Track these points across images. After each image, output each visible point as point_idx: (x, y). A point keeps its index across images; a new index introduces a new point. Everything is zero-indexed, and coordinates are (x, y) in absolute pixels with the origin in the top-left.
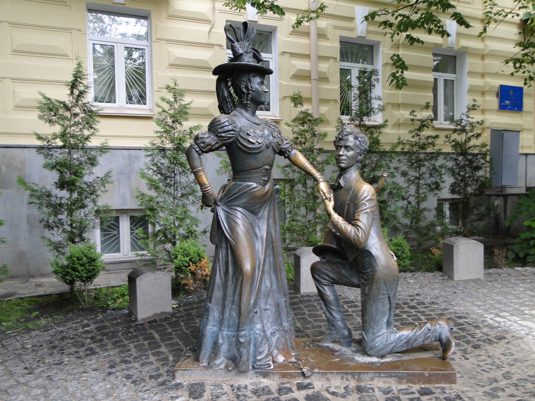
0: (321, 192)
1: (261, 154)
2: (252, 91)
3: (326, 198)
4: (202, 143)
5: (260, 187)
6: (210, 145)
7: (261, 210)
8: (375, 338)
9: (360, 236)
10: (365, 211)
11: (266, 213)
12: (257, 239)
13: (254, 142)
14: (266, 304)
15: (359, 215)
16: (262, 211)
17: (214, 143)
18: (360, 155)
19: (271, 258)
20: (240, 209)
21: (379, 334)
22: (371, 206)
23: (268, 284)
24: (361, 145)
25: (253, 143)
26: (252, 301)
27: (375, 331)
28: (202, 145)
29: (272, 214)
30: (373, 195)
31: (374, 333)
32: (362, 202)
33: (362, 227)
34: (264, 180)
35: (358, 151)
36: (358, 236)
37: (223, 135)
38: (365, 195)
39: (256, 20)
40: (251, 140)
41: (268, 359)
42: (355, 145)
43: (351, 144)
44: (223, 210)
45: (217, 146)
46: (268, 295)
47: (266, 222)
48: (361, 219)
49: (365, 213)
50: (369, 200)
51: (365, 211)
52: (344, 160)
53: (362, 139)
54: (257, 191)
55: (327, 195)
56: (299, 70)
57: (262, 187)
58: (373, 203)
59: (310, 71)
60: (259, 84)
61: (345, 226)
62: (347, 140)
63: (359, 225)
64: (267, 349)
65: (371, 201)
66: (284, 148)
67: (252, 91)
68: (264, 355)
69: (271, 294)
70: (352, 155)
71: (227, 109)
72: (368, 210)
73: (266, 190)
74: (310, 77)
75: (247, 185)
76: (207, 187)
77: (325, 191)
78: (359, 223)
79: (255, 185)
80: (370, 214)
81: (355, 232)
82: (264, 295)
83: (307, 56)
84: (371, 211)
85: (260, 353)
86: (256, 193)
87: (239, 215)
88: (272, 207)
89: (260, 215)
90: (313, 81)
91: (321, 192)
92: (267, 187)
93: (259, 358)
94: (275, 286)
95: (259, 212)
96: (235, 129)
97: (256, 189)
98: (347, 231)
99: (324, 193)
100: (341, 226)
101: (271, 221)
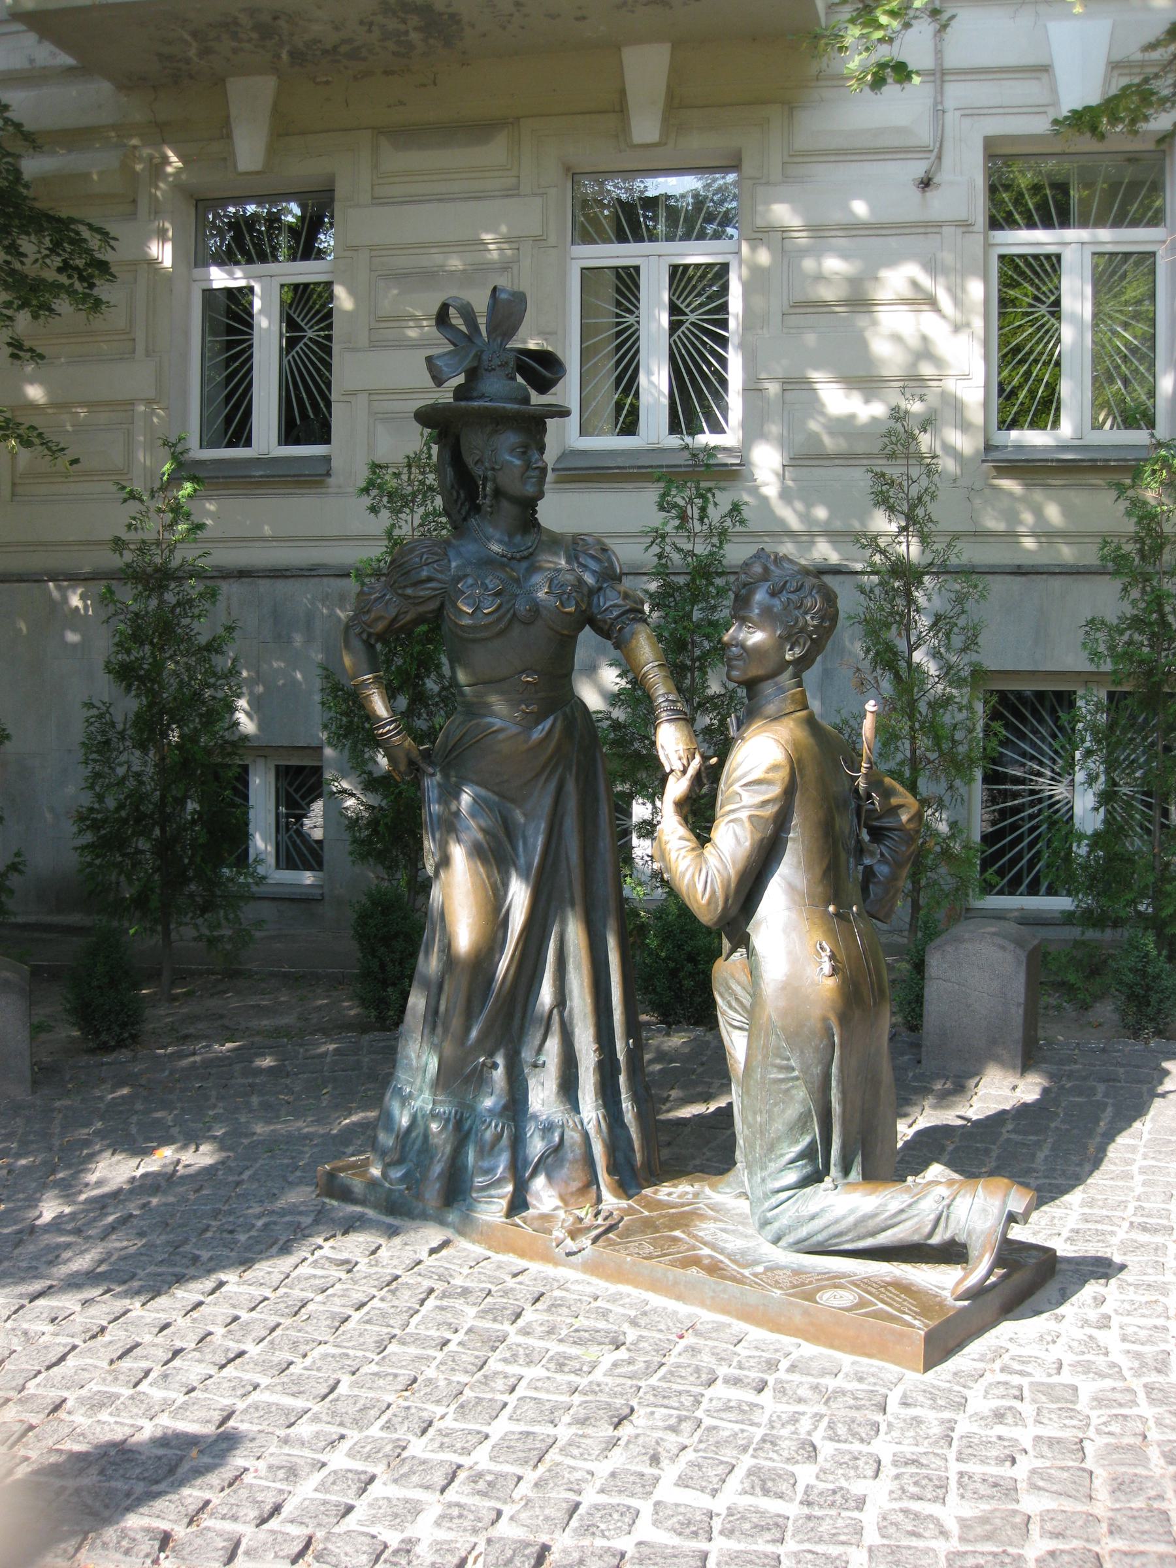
11: (547, 801)
30: (775, 768)
34: (524, 712)
37: (409, 591)
50: (759, 782)
65: (763, 787)
76: (383, 726)
80: (747, 824)
84: (750, 817)
88: (571, 787)
96: (440, 576)
97: (501, 736)
101: (571, 824)
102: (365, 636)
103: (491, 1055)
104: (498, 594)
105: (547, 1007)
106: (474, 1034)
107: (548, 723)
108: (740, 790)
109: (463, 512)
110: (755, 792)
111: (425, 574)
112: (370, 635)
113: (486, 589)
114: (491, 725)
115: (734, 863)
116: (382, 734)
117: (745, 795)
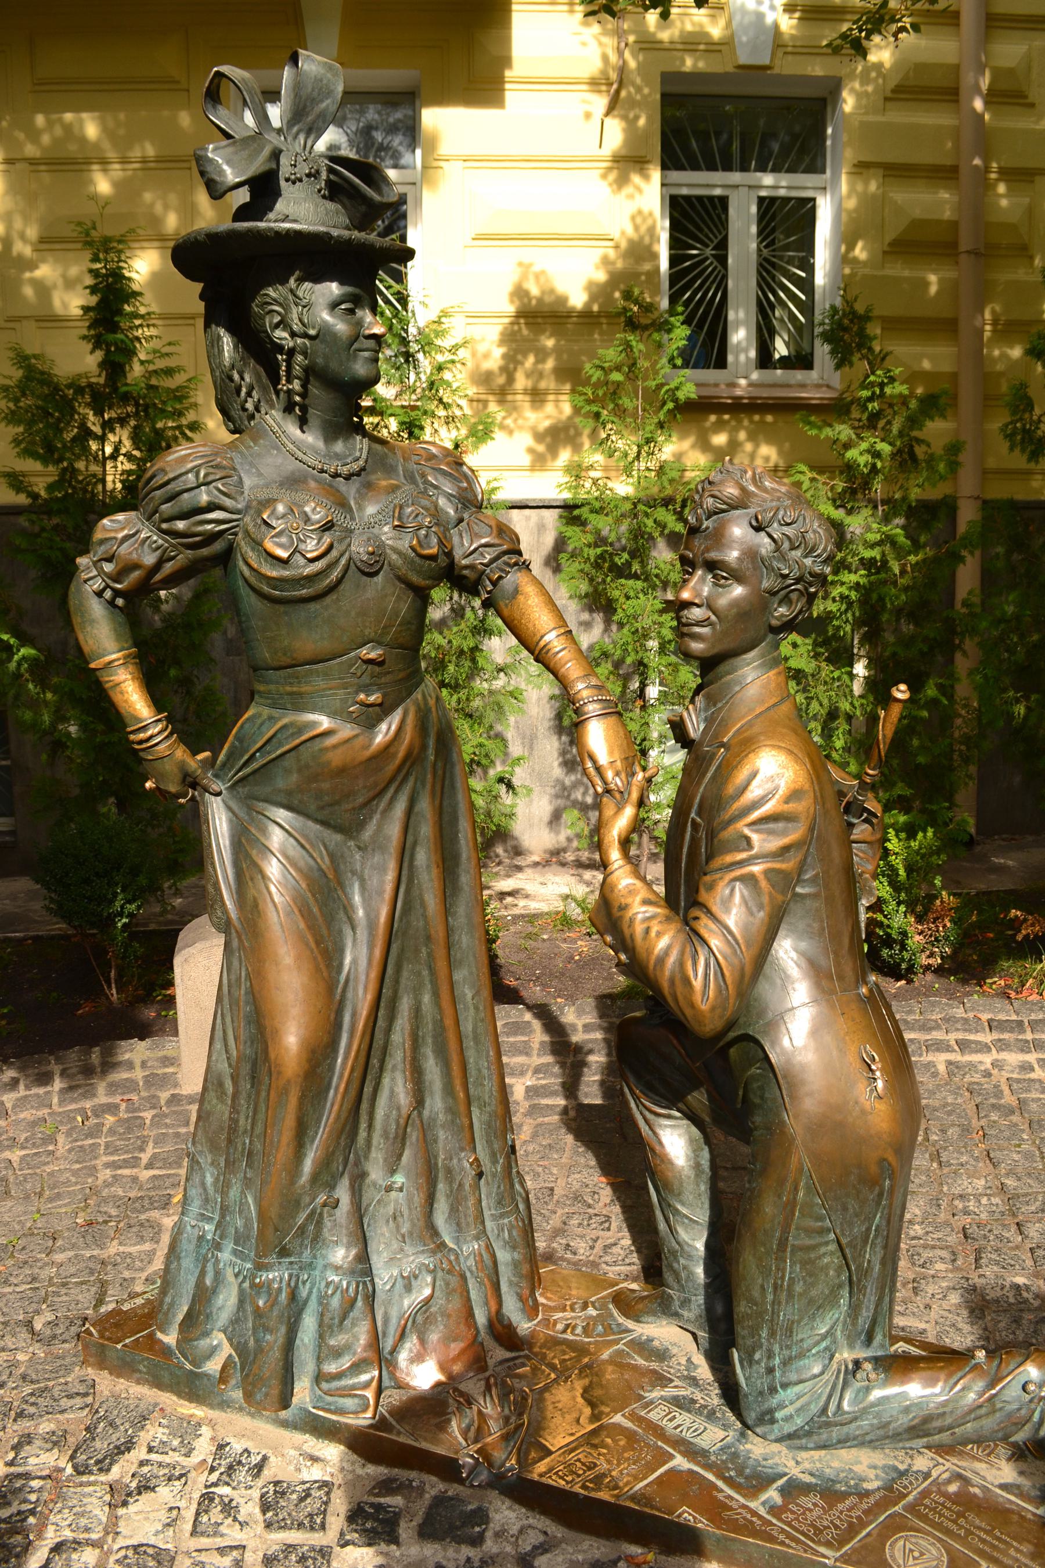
0: (589, 764)
1: (328, 600)
2: (306, 336)
3: (608, 791)
4: (109, 560)
5: (347, 731)
6: (136, 566)
7: (373, 812)
8: (773, 1390)
9: (698, 984)
10: (738, 873)
11: (394, 830)
12: (353, 929)
13: (284, 554)
14: (393, 1172)
15: (711, 887)
16: (377, 817)
17: (149, 559)
18: (786, 600)
19: (426, 998)
20: (282, 815)
21: (793, 1377)
22: (775, 844)
23: (404, 1099)
24: (783, 558)
25: (284, 562)
26: (308, 1166)
27: (777, 1361)
28: (108, 567)
29: (426, 830)
30: (794, 795)
31: (770, 1371)
32: (731, 829)
33: (715, 943)
34: (363, 704)
35: (765, 584)
36: (687, 982)
37: (181, 525)
38: (755, 791)
39: (766, 61)
40: (269, 545)
41: (364, 1377)
42: (751, 554)
43: (733, 555)
44: (229, 808)
45: (168, 567)
46: (401, 1138)
47: (392, 865)
48: (715, 909)
49: (741, 879)
51: (738, 873)
52: (698, 624)
53: (789, 531)
54: (335, 747)
55: (610, 775)
56: (917, 224)
57: (357, 730)
58: (784, 833)
59: (954, 225)
60: (334, 306)
61: (647, 931)
62: (718, 537)
63: (703, 932)
64: (363, 1339)
65: (781, 825)
66: (471, 567)
67: (306, 336)
68: (346, 1362)
69: (413, 1135)
70: (735, 603)
71: (244, 415)
72: (756, 869)
73: (379, 739)
74: (954, 245)
75: (292, 724)
76: (144, 728)
77: (603, 759)
78: (705, 926)
79: (325, 722)
80: (764, 884)
81: (681, 963)
82: (385, 1134)
83: (945, 174)
84: (766, 872)
85: (337, 1353)
86: (330, 755)
87: (276, 838)
88: (425, 805)
89: (367, 834)
90: (963, 258)
91: (589, 764)
92: (383, 732)
93: (331, 1368)
94: (436, 1104)
95: (362, 825)
96: (228, 502)
98: (649, 951)
99: (598, 769)
100: (632, 921)
101: (423, 857)
102: (108, 594)
103: (332, 1187)
104: (328, 527)
105: (405, 1111)
106: (308, 1166)
107: (396, 718)
108: (747, 831)
109: (250, 406)
110: (771, 832)
111: (204, 497)
112: (117, 593)
113: (307, 520)
114: (314, 724)
115: (748, 945)
116: (141, 742)
117: (755, 837)
